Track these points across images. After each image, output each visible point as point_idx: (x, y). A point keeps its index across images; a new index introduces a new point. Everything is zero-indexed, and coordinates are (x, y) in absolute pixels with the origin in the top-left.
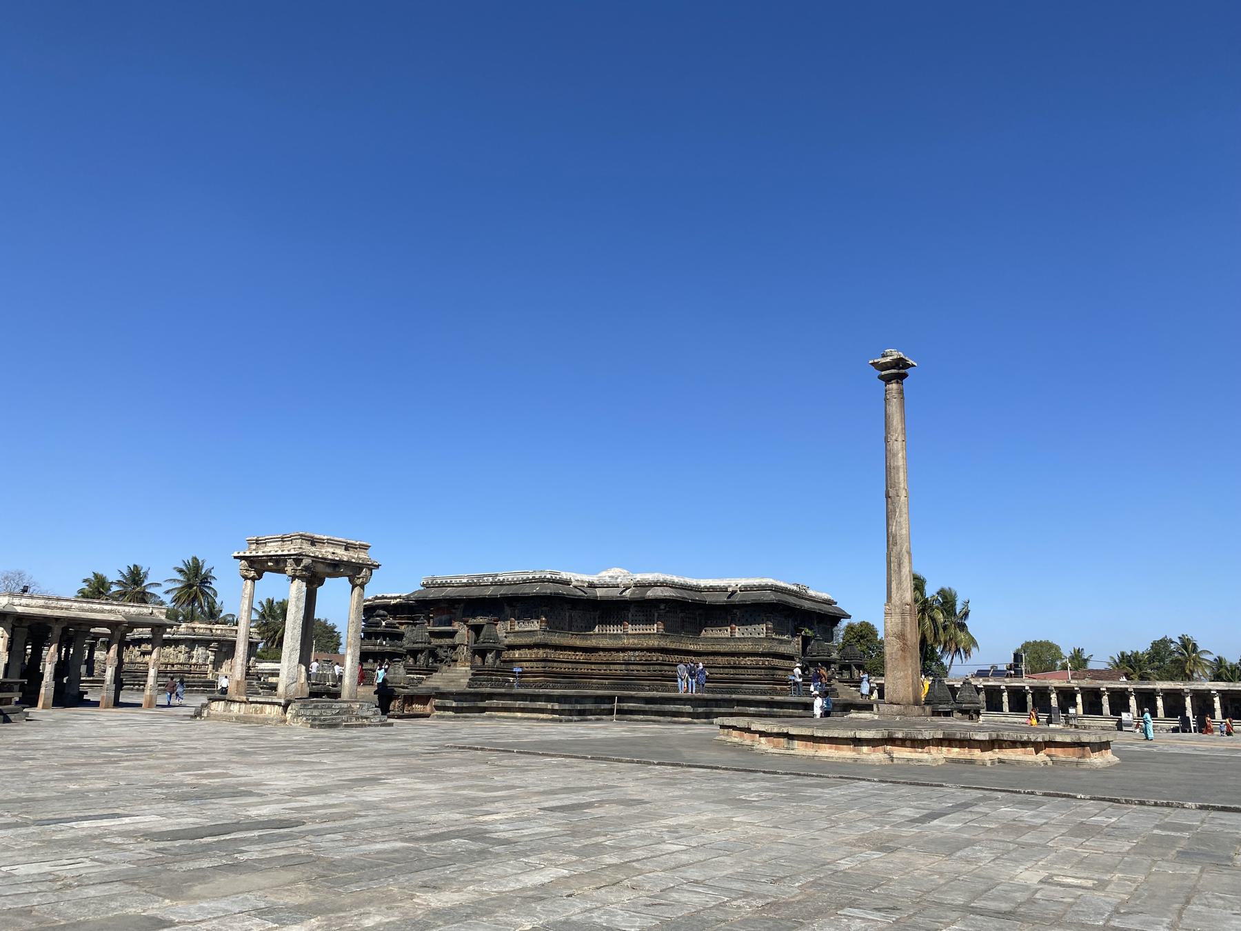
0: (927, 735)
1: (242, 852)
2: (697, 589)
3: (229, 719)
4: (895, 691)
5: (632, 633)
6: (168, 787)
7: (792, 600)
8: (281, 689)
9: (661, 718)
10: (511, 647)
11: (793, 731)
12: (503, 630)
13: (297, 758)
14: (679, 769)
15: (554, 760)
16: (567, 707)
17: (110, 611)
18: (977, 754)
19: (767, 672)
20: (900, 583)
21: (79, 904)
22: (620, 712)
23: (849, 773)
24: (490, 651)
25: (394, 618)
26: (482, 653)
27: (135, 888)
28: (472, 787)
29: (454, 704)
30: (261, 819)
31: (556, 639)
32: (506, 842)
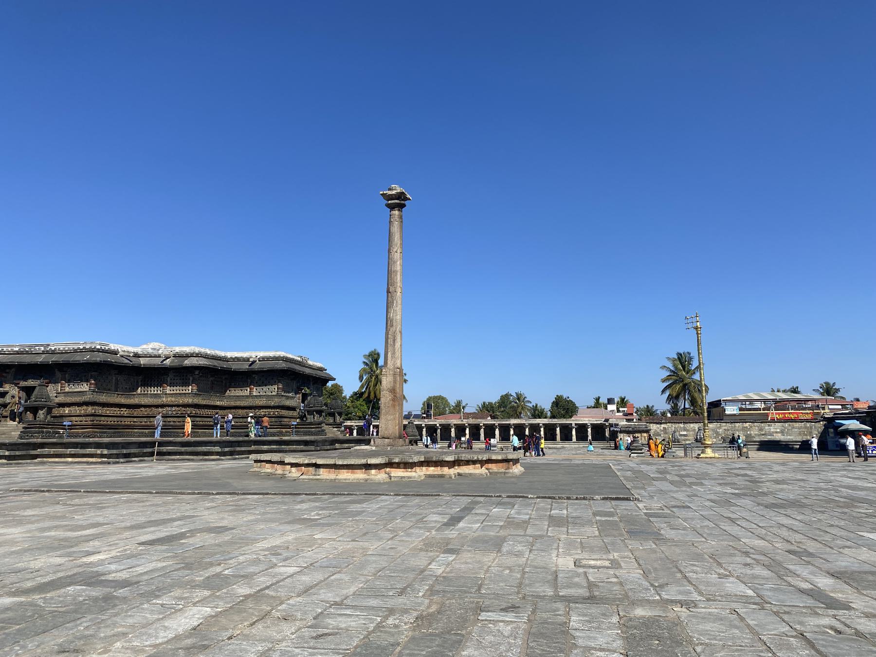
0: (416, 459)
4: (386, 429)
5: (169, 393)
7: (297, 368)
9: (195, 457)
11: (320, 462)
12: (54, 391)
14: (237, 497)
15: (124, 497)
16: (115, 452)
18: (446, 470)
19: (276, 419)
20: (394, 353)
22: (160, 454)
23: (371, 491)
24: (42, 408)
26: (34, 410)
28: (56, 527)
29: (7, 453)
31: (103, 398)
32: (125, 584)
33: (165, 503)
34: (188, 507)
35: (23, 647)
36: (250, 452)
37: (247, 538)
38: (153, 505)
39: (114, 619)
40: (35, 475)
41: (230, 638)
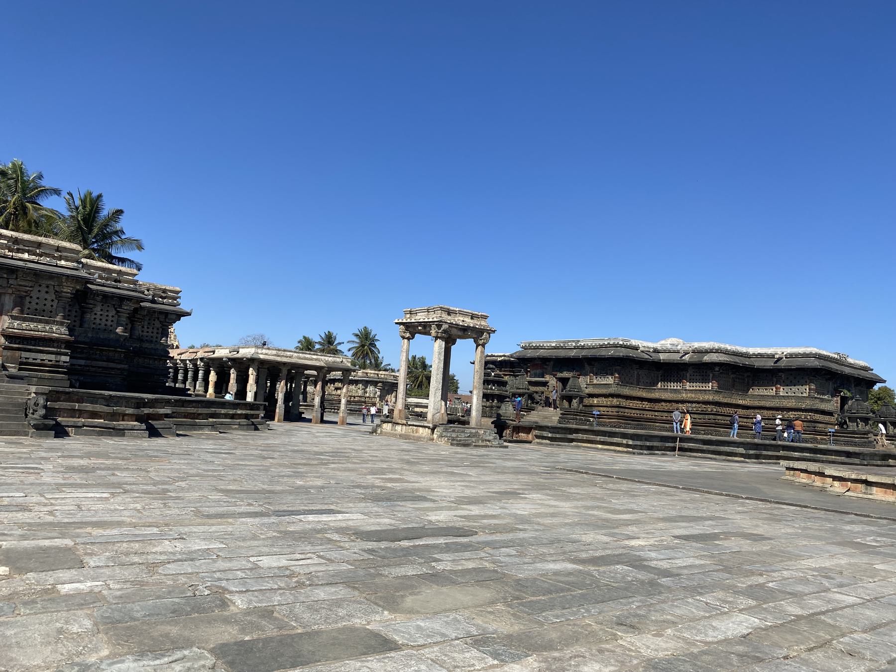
1: (436, 560)
2: (746, 356)
3: (395, 435)
5: (689, 389)
6: (365, 487)
7: (834, 366)
8: (429, 416)
9: (717, 457)
10: (591, 396)
11: (871, 479)
13: (450, 469)
14: (769, 505)
15: (653, 488)
16: (638, 443)
17: (316, 360)
21: (313, 607)
22: (681, 449)
24: (575, 397)
25: (500, 371)
26: (569, 399)
27: (356, 593)
28: (599, 508)
29: (550, 435)
30: (441, 525)
31: (626, 391)
32: (666, 573)
33: (693, 500)
34: (717, 507)
35: (588, 611)
36: (779, 458)
37: (789, 553)
38: (681, 500)
39: (663, 605)
40: (573, 457)
41: (786, 658)
